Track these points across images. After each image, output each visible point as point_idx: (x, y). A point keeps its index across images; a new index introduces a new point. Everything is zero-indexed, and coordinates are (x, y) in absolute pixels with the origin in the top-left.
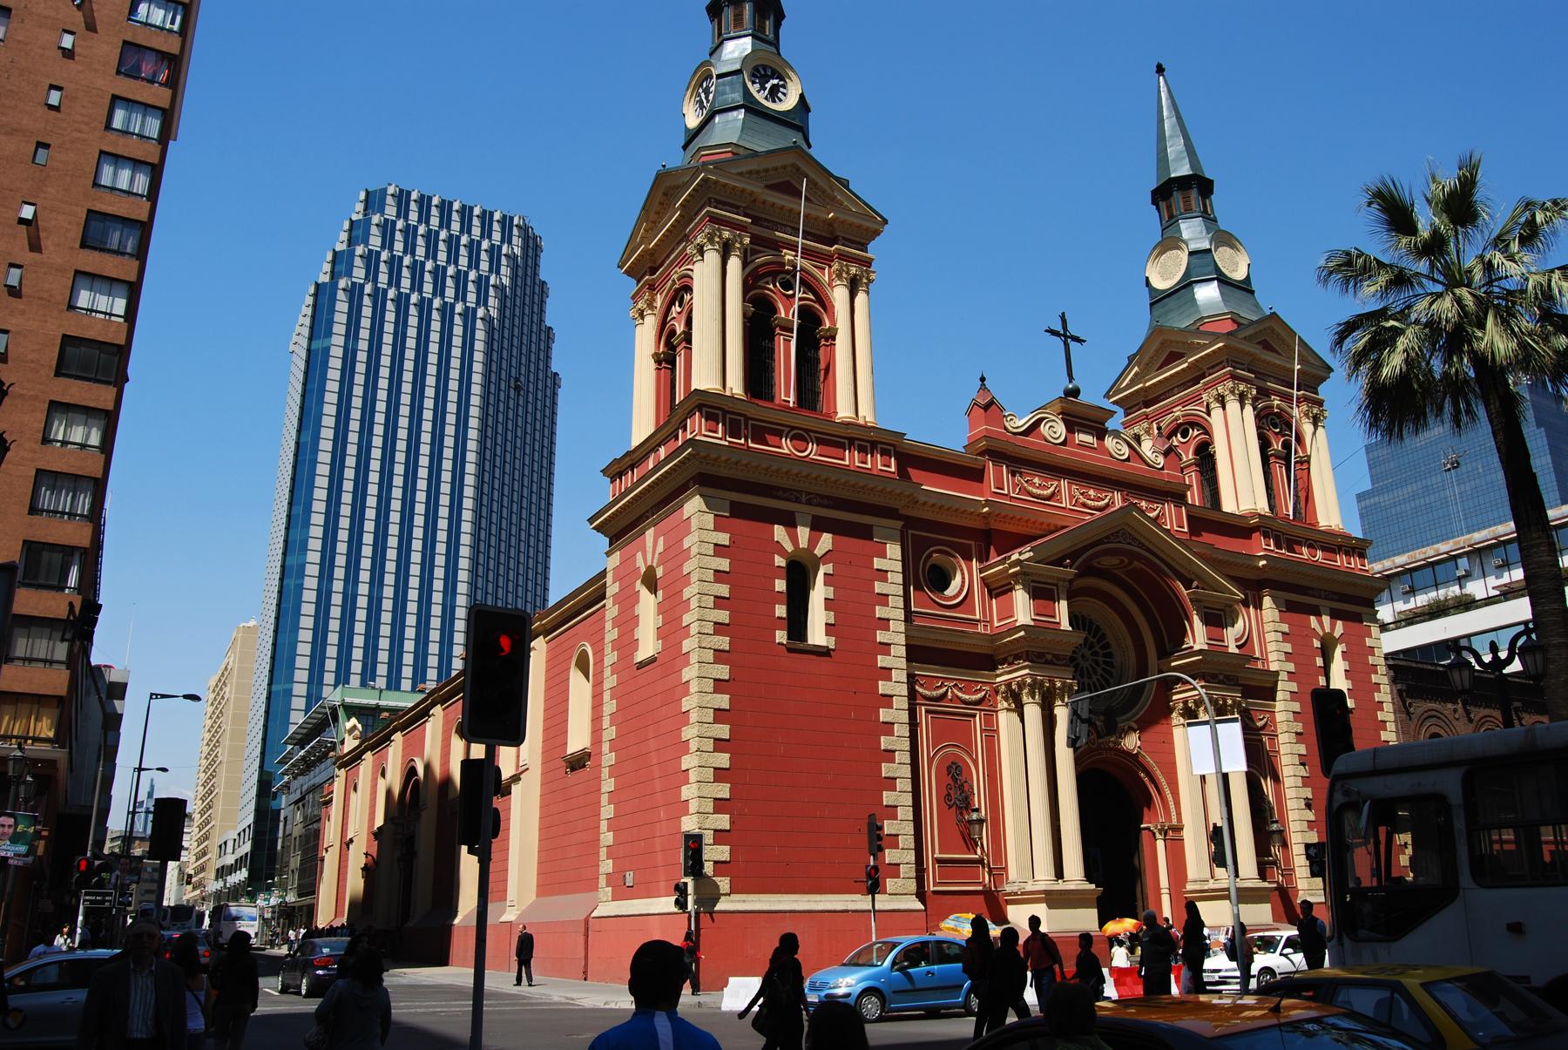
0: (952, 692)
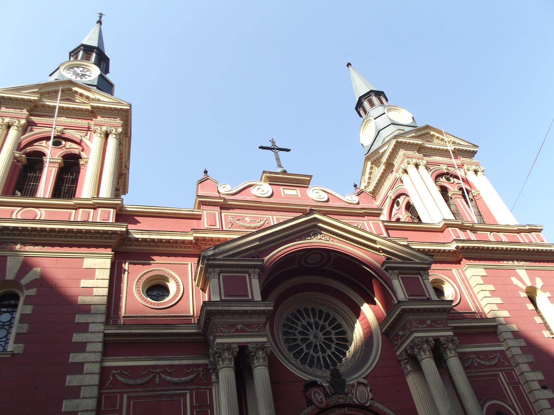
0: (160, 378)
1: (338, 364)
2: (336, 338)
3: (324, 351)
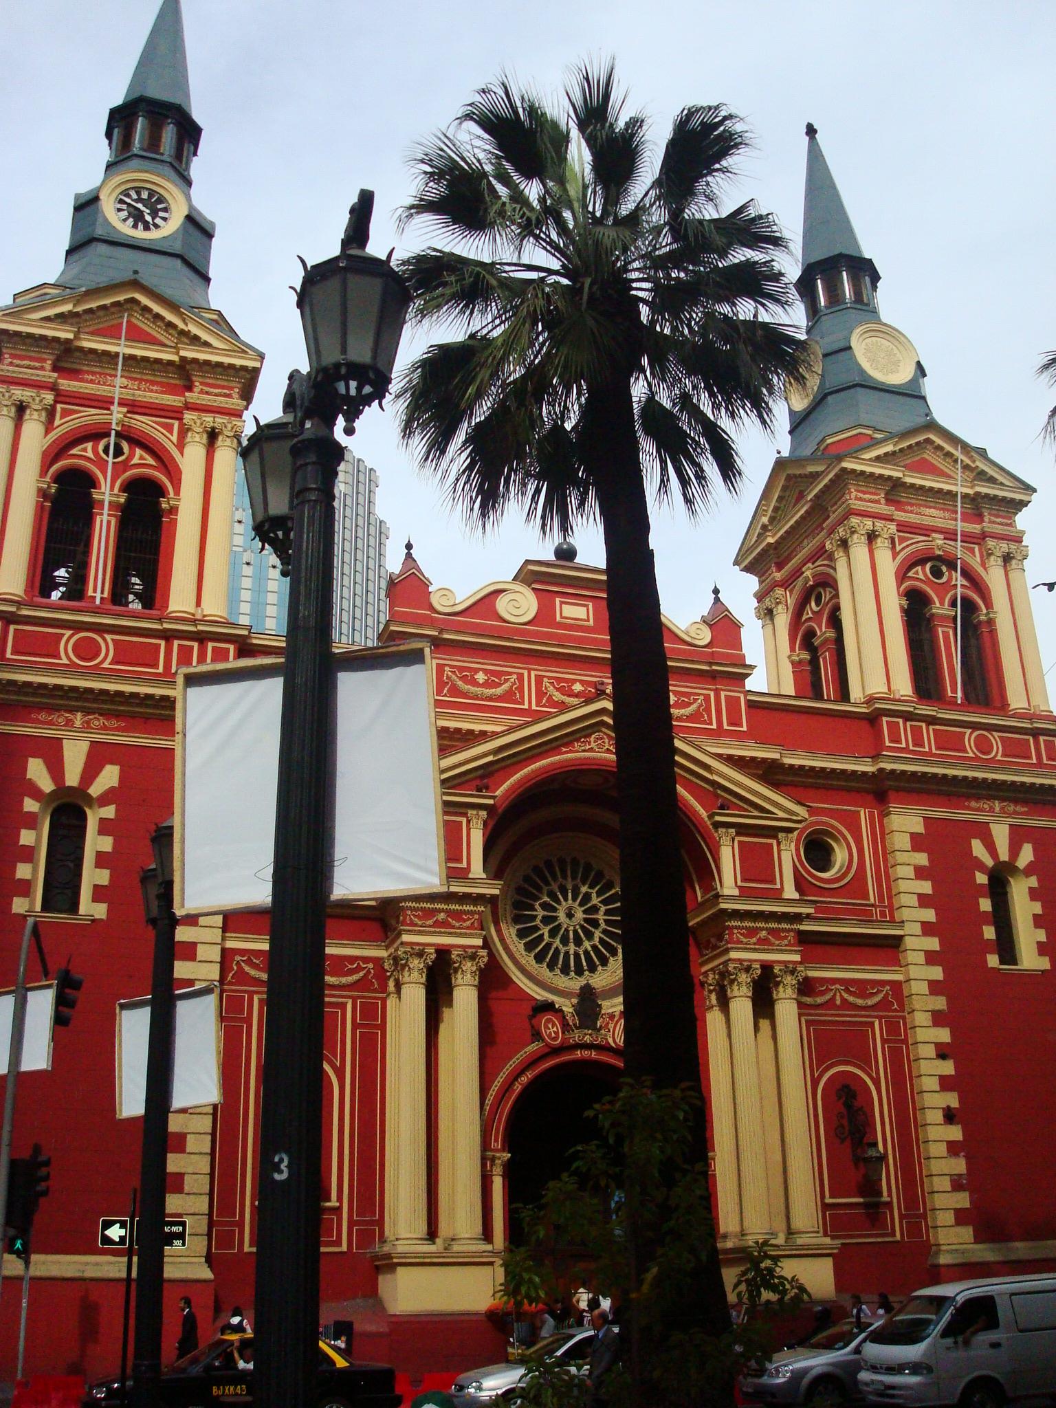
2: (605, 920)
3: (578, 942)
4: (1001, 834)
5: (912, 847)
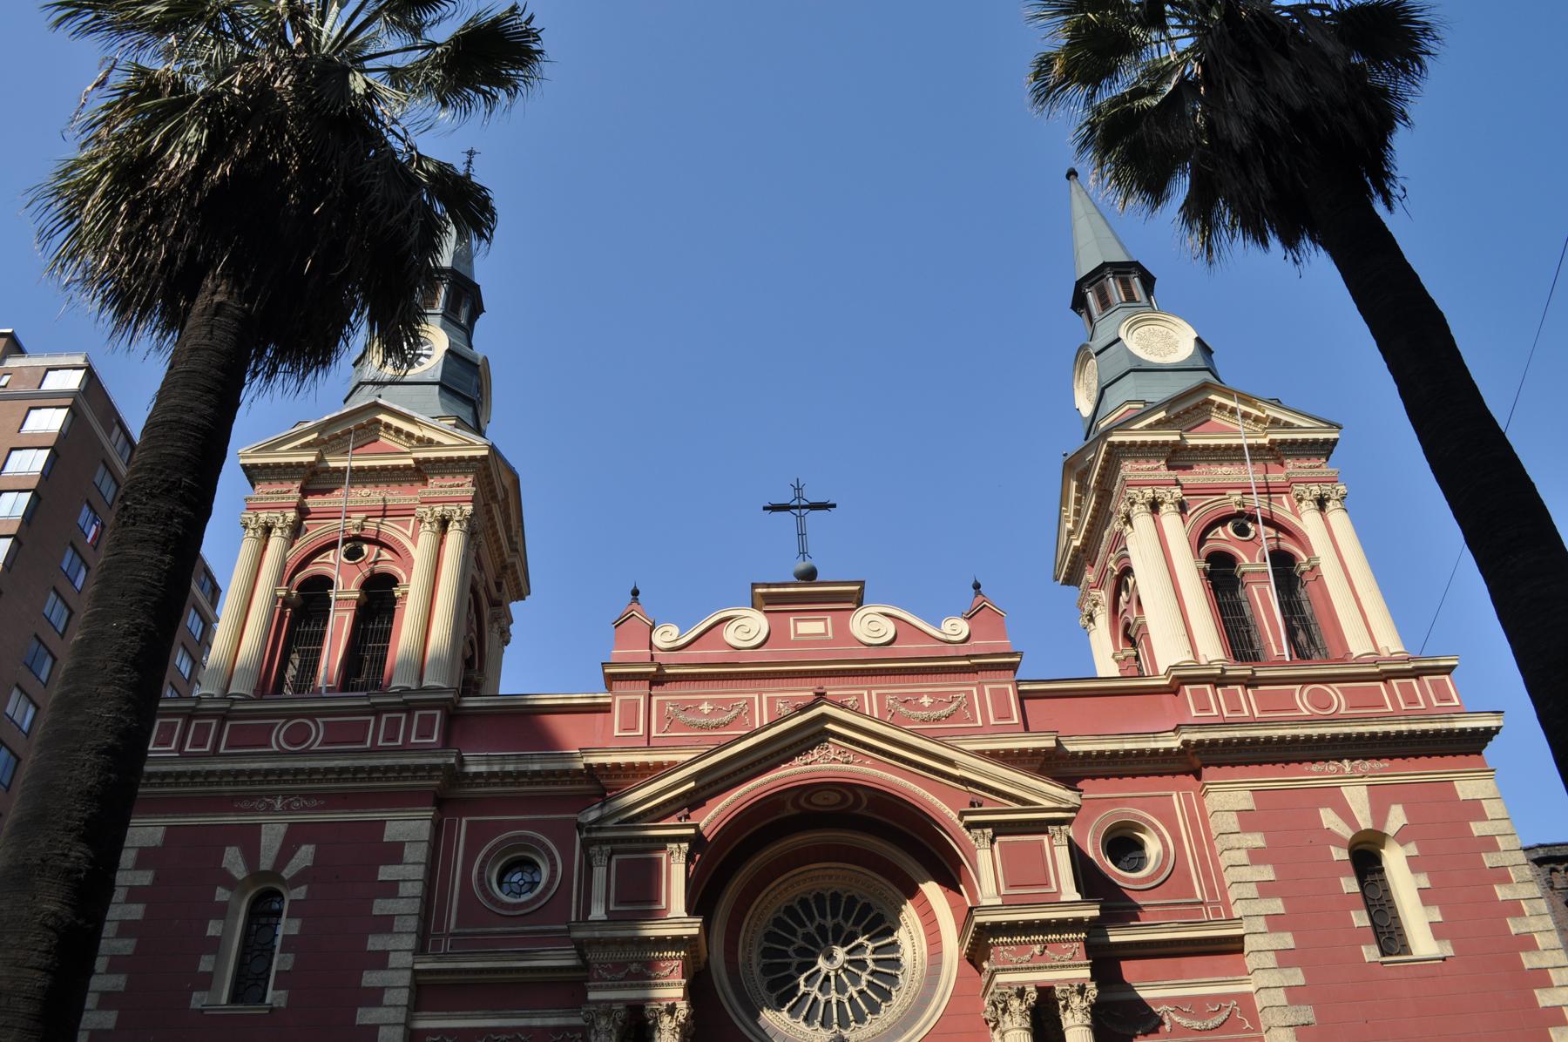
1: (869, 1017)
3: (841, 988)
4: (1357, 797)
5: (1241, 827)
